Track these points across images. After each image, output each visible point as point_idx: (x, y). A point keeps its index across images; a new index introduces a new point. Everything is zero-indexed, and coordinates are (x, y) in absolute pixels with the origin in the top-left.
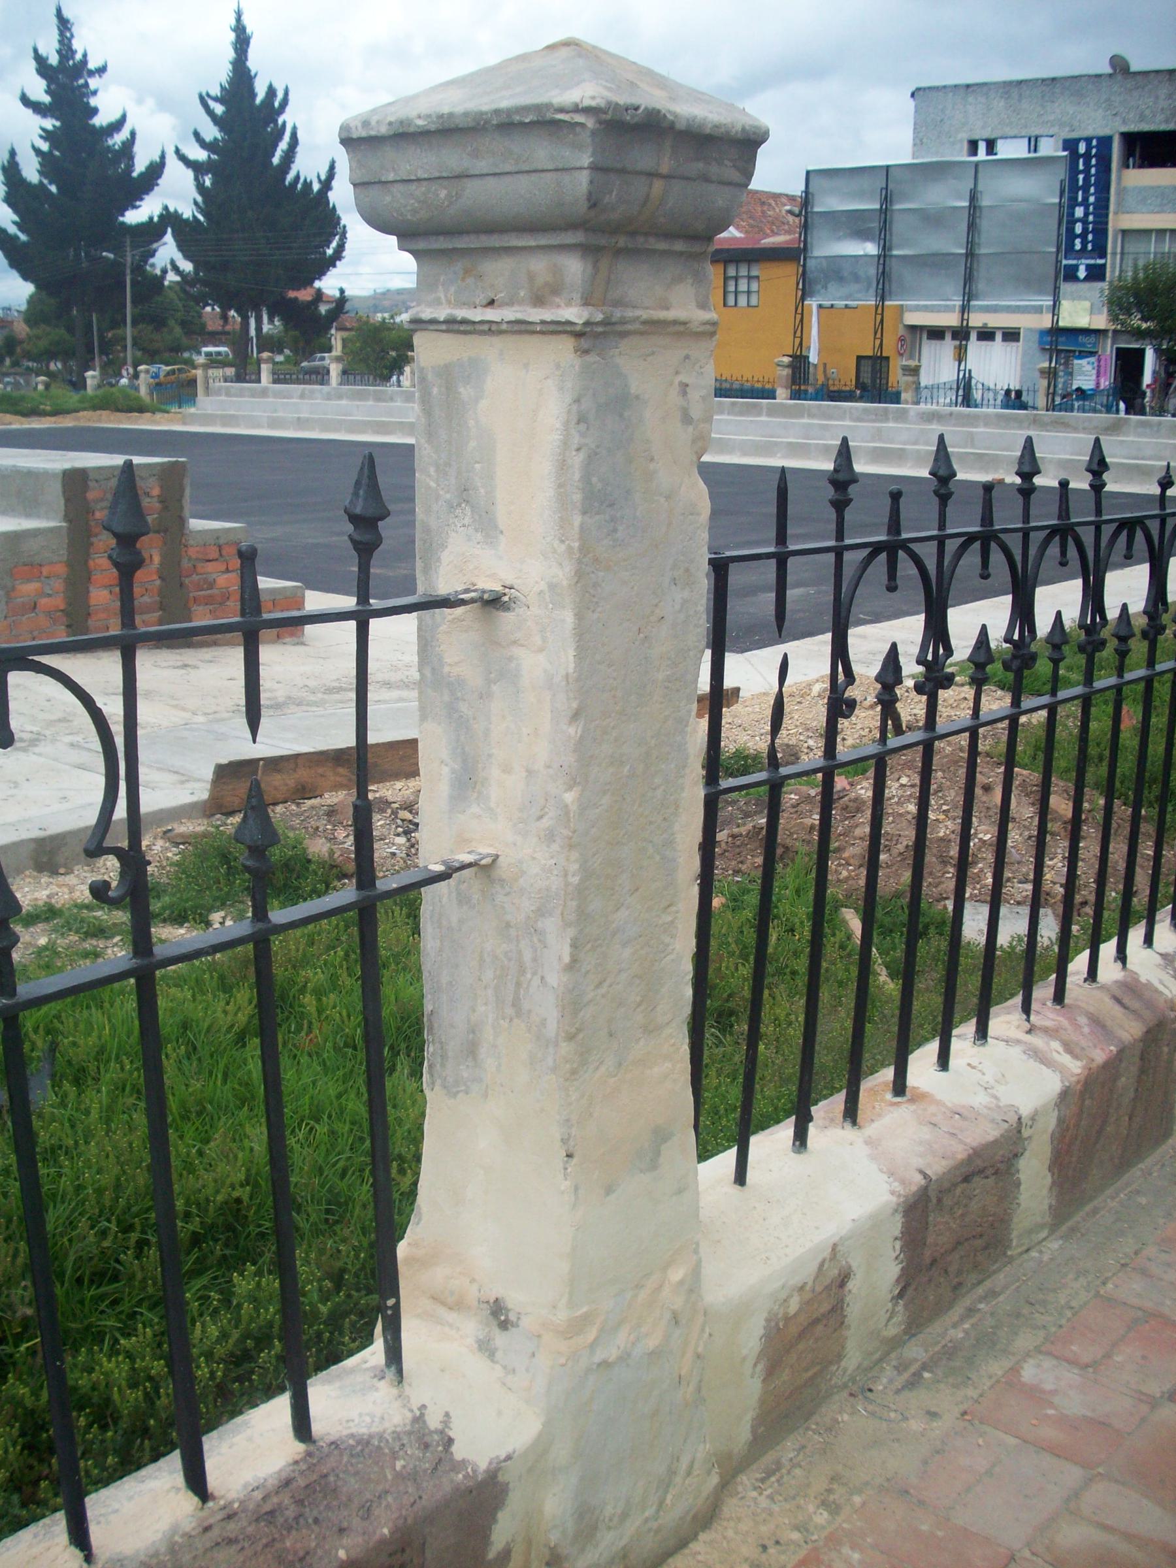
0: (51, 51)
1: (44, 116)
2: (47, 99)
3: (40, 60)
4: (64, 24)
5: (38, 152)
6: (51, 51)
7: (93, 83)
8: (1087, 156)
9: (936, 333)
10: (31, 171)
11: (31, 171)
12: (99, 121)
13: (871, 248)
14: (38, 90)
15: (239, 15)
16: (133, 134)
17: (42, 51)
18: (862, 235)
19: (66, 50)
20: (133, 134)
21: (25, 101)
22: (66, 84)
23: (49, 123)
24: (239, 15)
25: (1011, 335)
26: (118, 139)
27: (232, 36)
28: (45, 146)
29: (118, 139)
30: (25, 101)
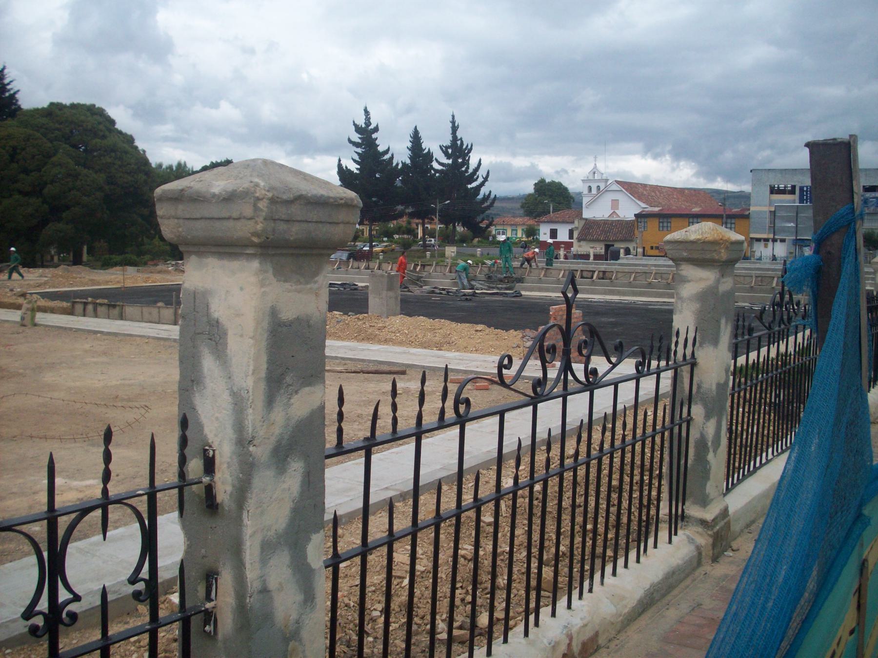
0: (361, 122)
1: (357, 147)
2: (360, 141)
3: (355, 124)
4: (366, 112)
5: (355, 161)
6: (361, 122)
7: (374, 136)
8: (807, 191)
9: (758, 240)
10: (354, 167)
11: (354, 167)
12: (381, 149)
13: (792, 224)
14: (356, 138)
15: (453, 117)
16: (392, 155)
17: (357, 122)
18: (790, 222)
19: (368, 122)
20: (392, 155)
21: (350, 141)
22: (366, 135)
23: (359, 150)
24: (453, 117)
25: (783, 241)
26: (386, 157)
27: (451, 125)
28: (357, 158)
29: (386, 157)
30: (350, 141)
